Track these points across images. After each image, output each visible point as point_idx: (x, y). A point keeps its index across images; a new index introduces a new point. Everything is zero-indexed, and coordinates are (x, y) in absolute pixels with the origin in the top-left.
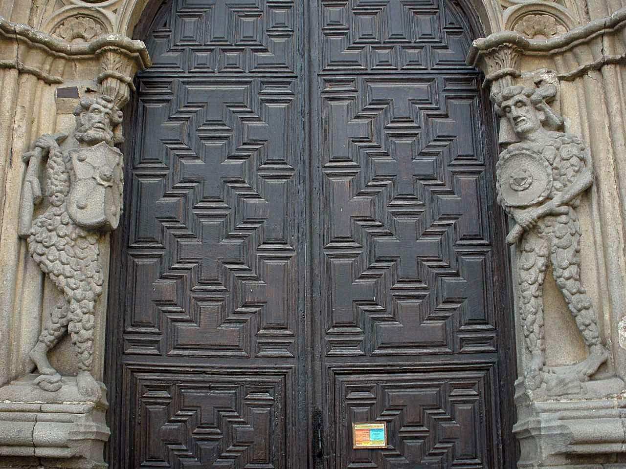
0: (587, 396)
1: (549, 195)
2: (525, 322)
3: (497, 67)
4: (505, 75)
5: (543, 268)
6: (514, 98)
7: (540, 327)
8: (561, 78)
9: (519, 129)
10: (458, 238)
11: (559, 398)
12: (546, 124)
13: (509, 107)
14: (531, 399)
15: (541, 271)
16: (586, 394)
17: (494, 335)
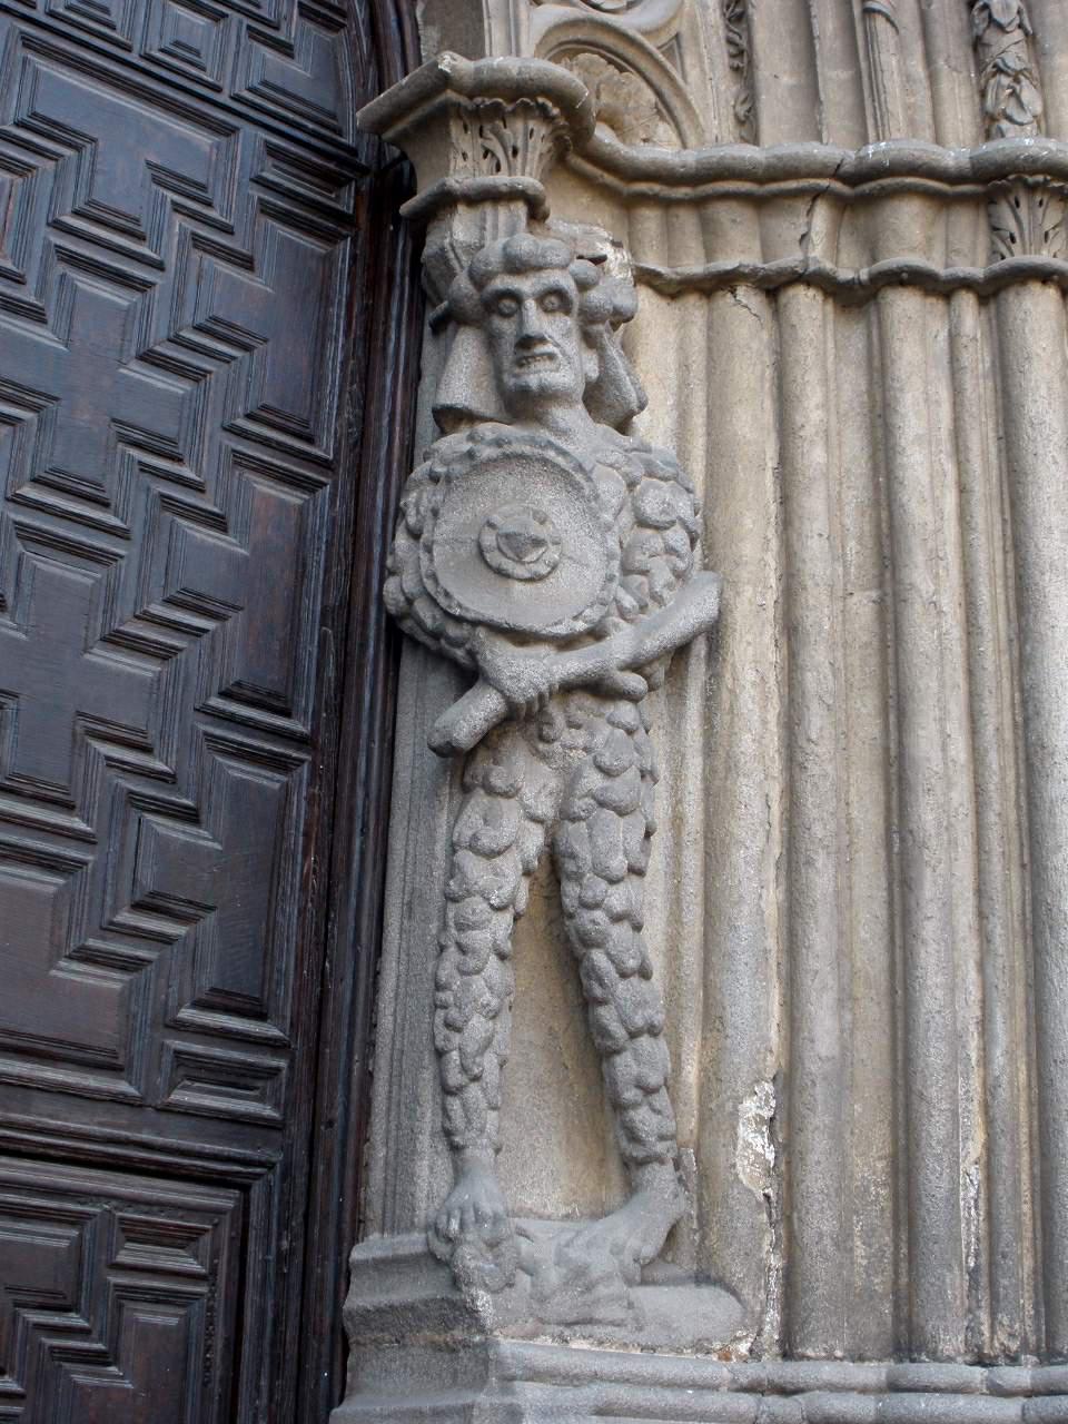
0: (643, 1338)
2: (456, 1039)
4: (513, 195)
6: (544, 274)
9: (533, 381)
10: (215, 689)
11: (567, 1332)
13: (516, 297)
14: (489, 1323)
16: (640, 1329)
17: (283, 1064)
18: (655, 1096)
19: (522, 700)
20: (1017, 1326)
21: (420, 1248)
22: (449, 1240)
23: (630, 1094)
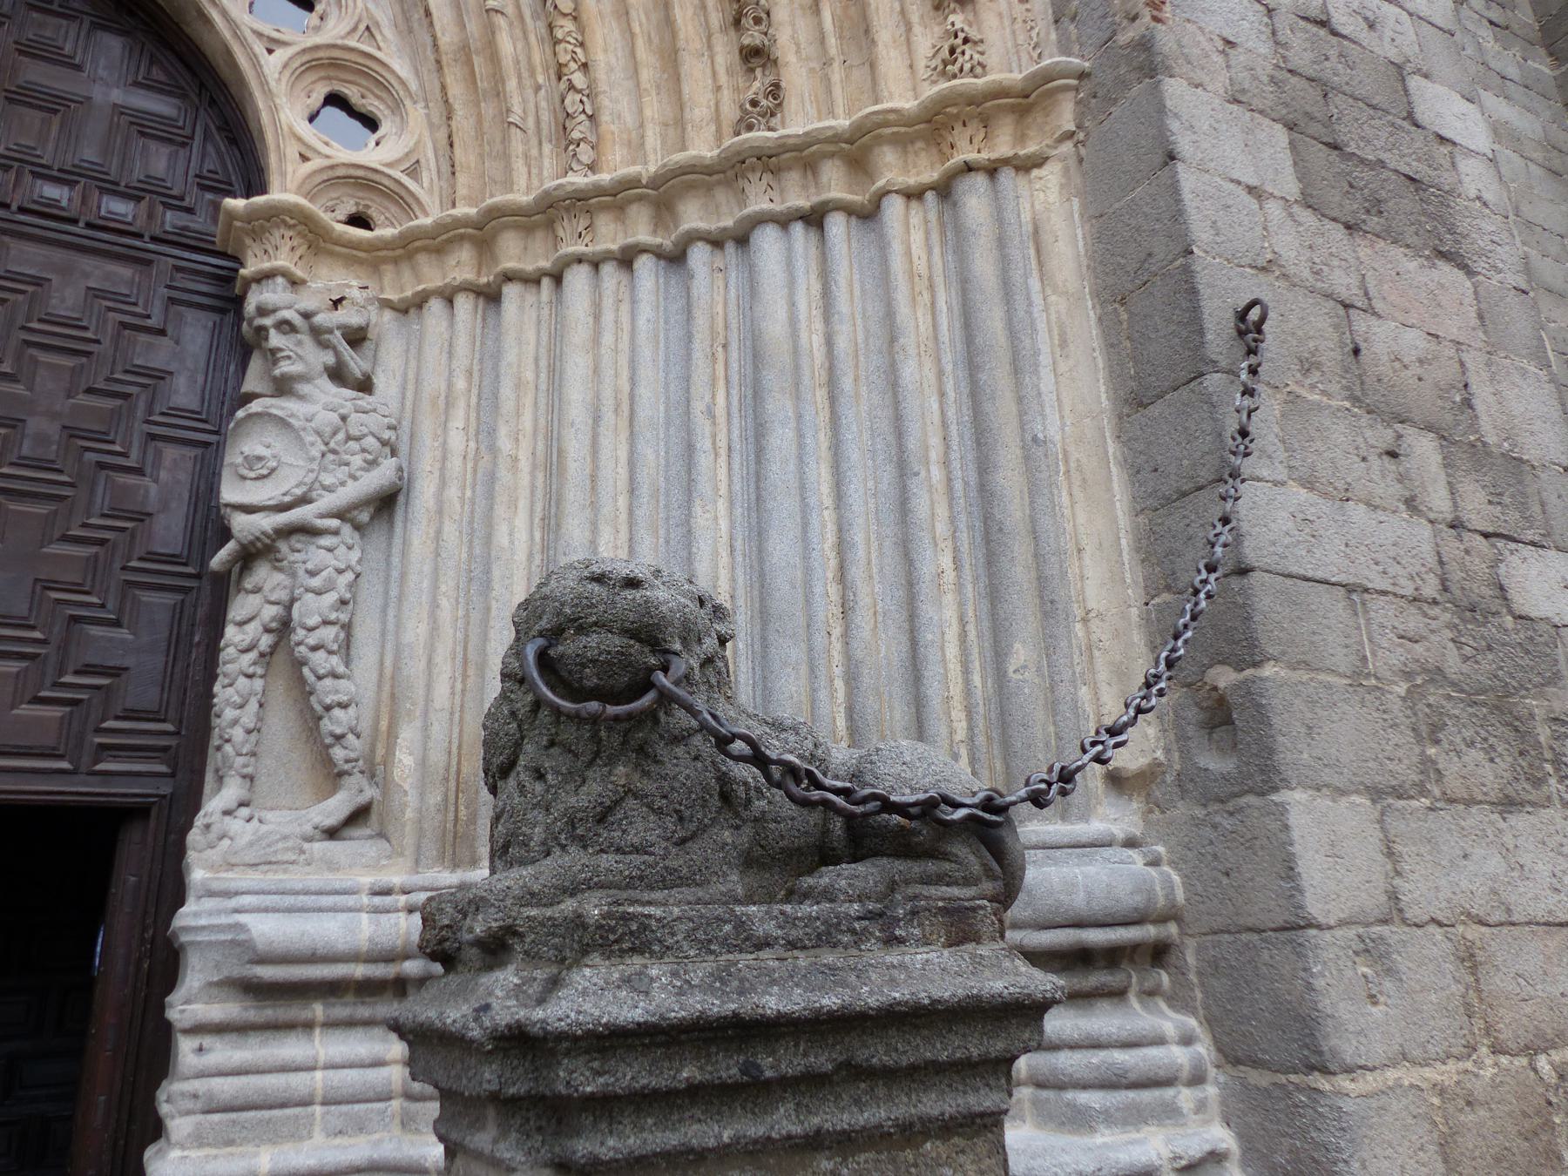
1: (305, 494)
3: (265, 257)
5: (274, 625)
8: (386, 304)
9: (277, 372)
12: (337, 374)
15: (267, 630)
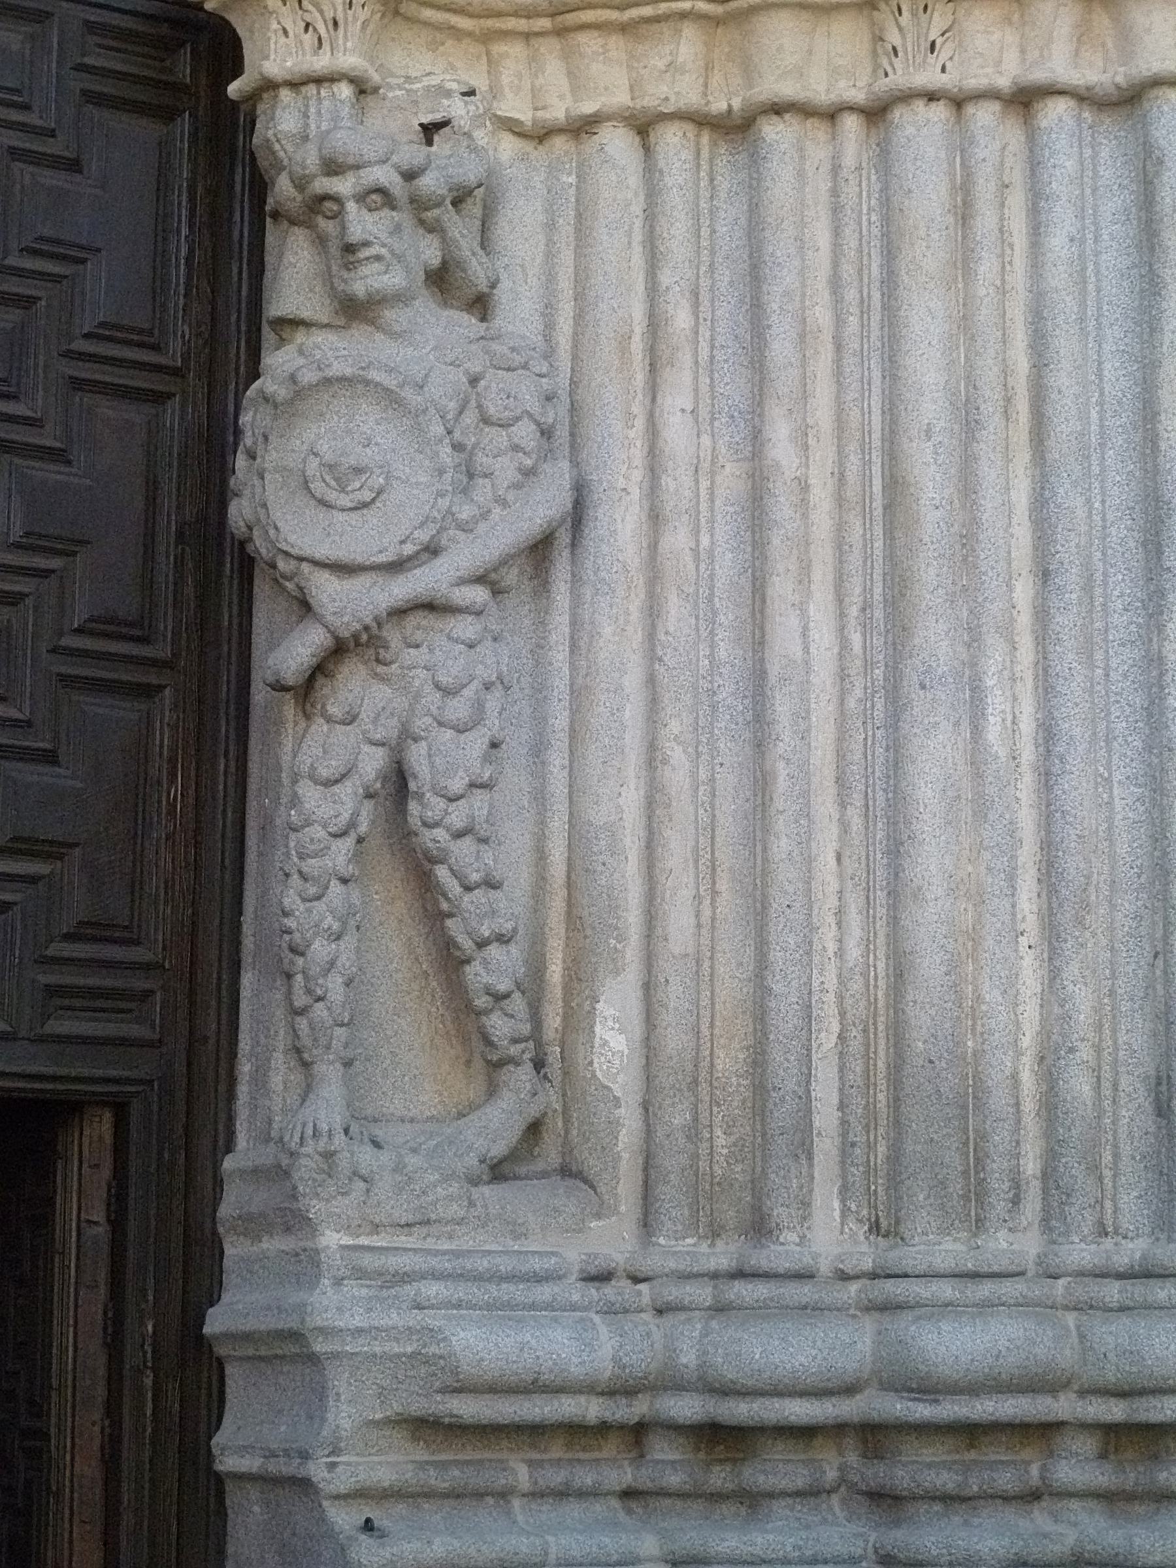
2: (300, 961)
3: (309, 39)
6: (362, 172)
7: (348, 984)
9: (359, 288)
15: (369, 796)
18: (507, 1001)
19: (347, 634)
20: (865, 1212)
21: (270, 1161)
22: (292, 1154)
23: (481, 1002)
